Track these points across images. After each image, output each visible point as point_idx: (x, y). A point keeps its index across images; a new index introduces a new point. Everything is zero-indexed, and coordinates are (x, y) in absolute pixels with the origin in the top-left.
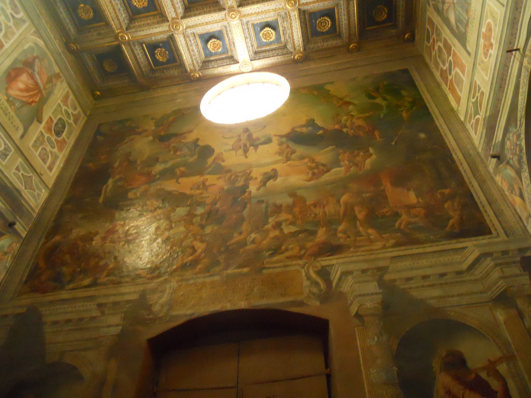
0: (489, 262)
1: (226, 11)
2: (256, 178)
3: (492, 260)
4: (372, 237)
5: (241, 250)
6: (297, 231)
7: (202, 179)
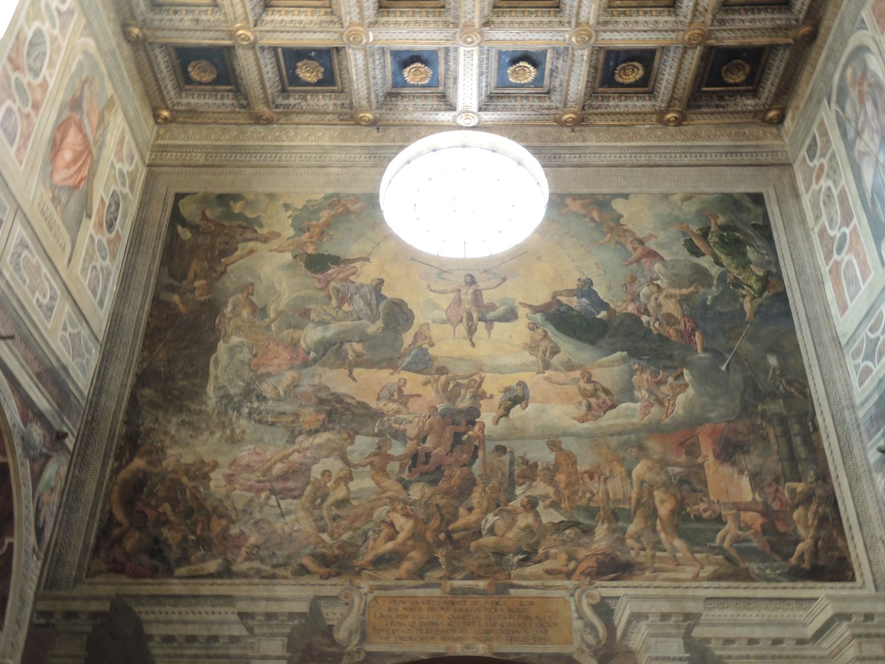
0: (843, 630)
1: (458, 29)
2: (491, 397)
3: (850, 627)
4: (679, 555)
5: (473, 544)
6: (562, 522)
7: (395, 379)
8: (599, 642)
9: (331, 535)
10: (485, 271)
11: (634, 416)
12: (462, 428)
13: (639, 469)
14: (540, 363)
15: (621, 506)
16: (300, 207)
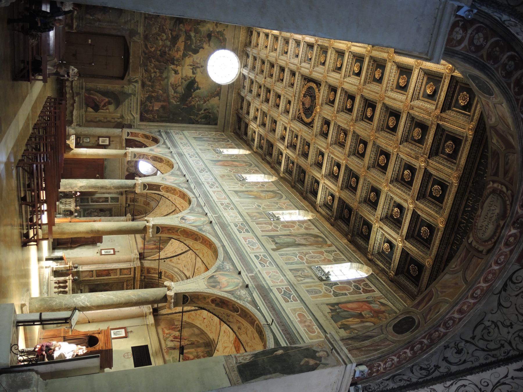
0: (132, 118)
13: (161, 92)
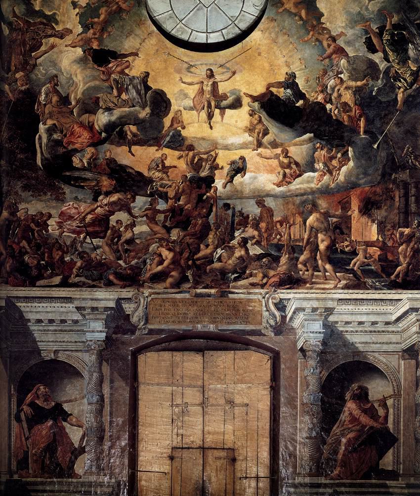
2: (222, 168)
8: (276, 323)
9: (125, 262)
10: (221, 66)
11: (312, 182)
12: (203, 191)
13: (311, 219)
14: (255, 142)
15: (298, 244)
16: (84, 5)
